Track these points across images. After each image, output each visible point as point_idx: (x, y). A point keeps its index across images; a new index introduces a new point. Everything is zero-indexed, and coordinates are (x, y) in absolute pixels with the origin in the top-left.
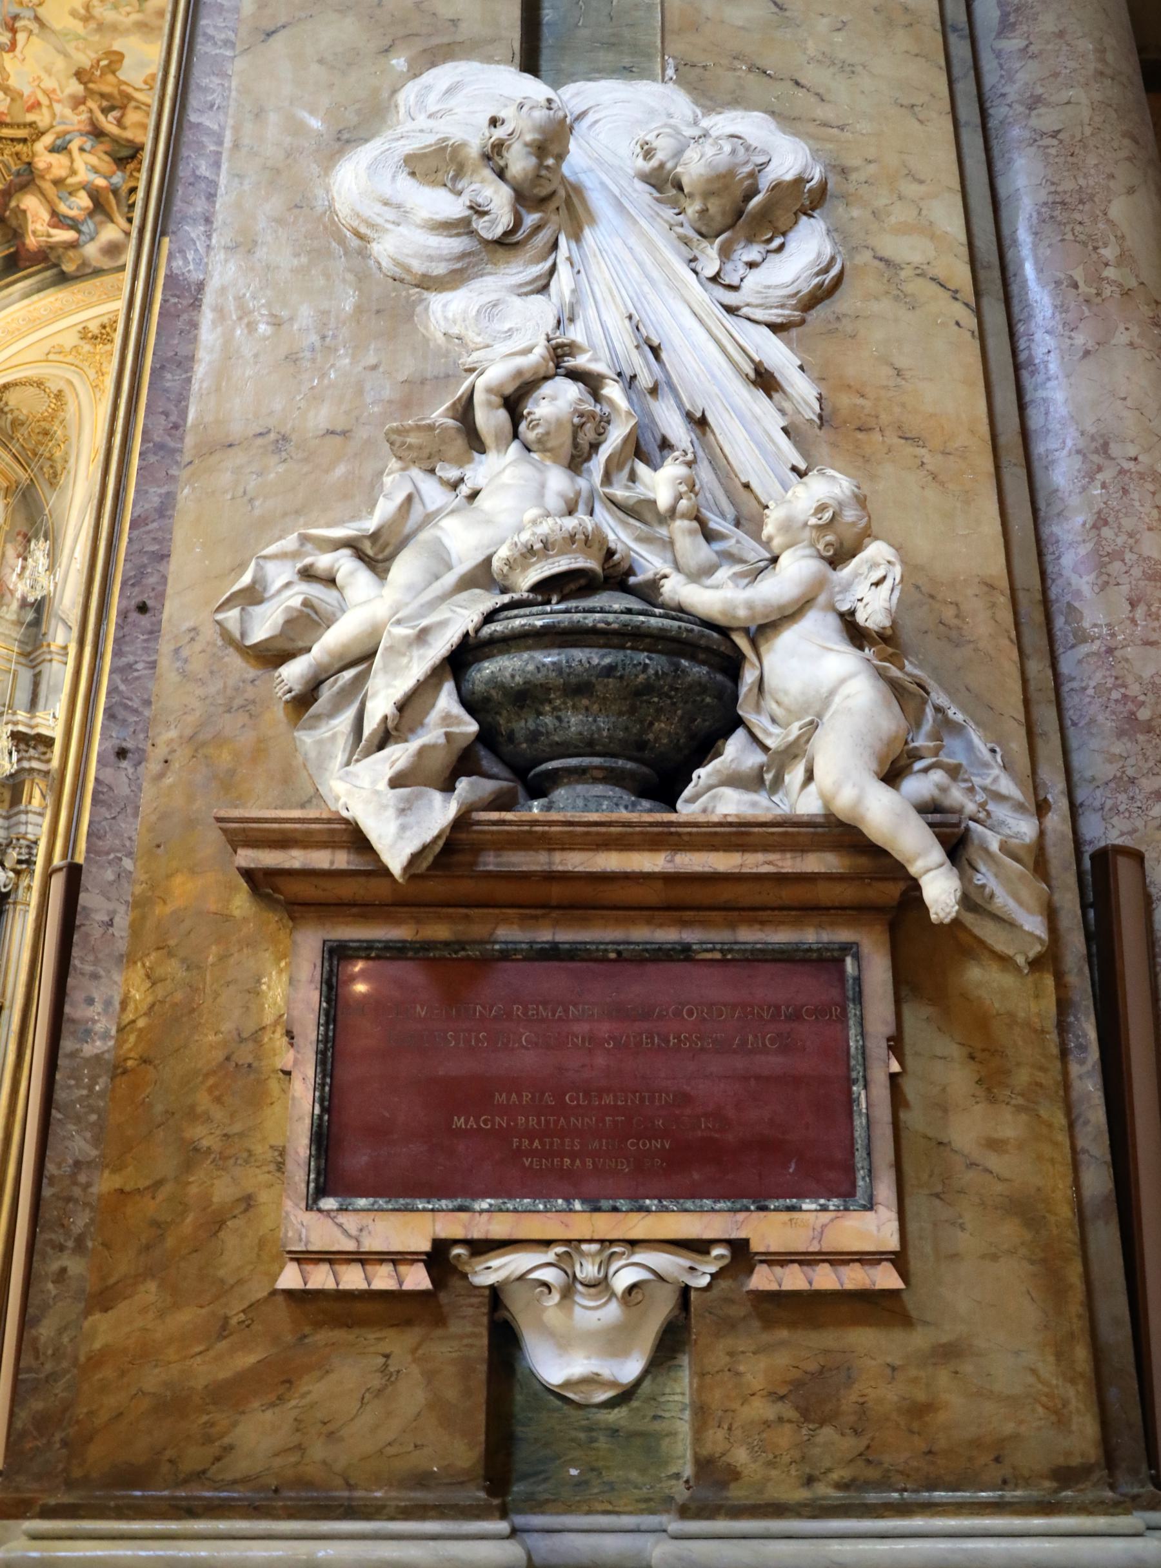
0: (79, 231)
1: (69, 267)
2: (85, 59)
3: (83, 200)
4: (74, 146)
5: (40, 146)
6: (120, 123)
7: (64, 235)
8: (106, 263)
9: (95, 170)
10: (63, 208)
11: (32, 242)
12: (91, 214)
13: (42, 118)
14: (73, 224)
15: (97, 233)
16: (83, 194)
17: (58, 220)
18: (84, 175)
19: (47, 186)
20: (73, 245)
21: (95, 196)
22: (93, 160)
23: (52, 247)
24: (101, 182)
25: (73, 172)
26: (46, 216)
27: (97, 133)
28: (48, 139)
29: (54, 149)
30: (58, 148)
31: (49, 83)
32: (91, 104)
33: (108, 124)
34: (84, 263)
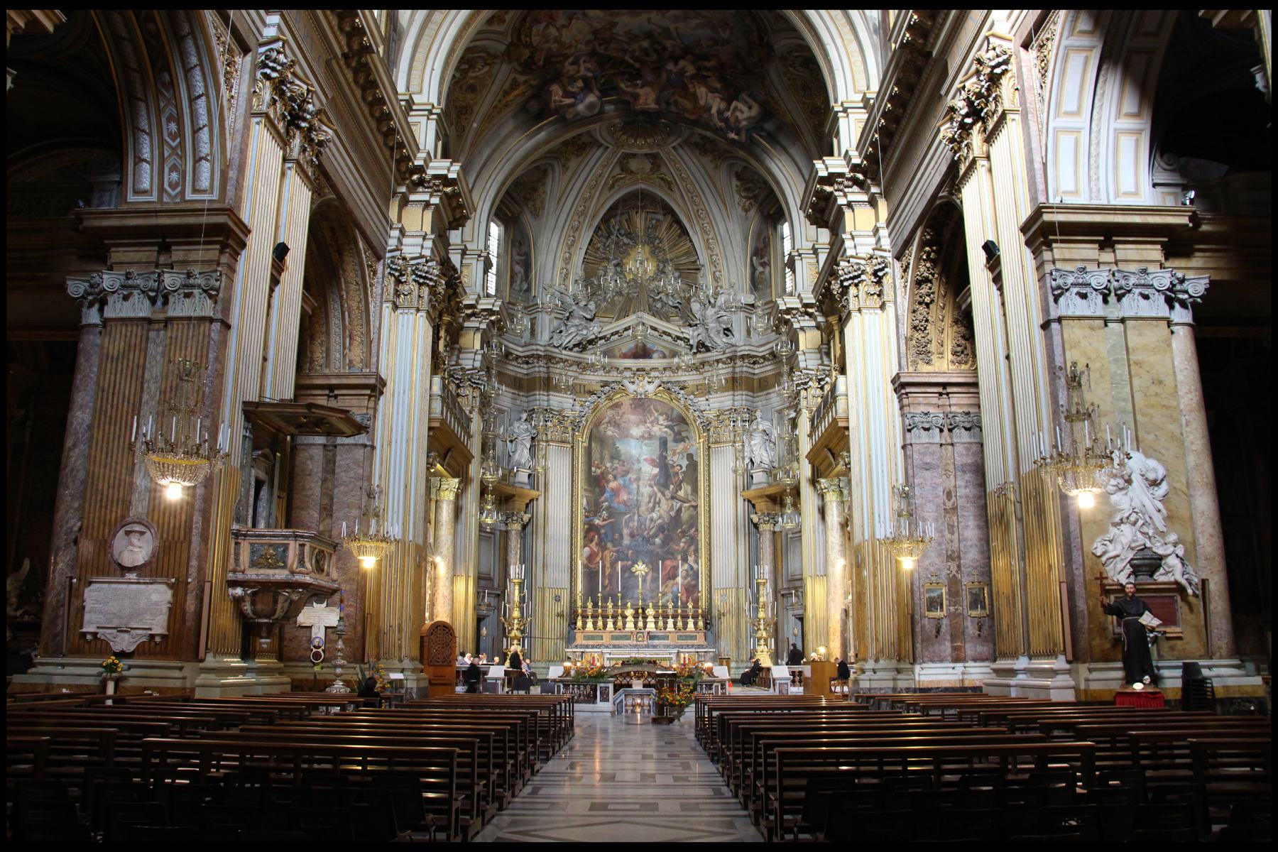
0: (575, 98)
1: (569, 116)
2: (598, 26)
3: (580, 84)
4: (581, 61)
5: (566, 64)
6: (606, 49)
7: (569, 101)
8: (588, 114)
9: (588, 70)
10: (570, 88)
11: (553, 105)
12: (582, 89)
13: (569, 52)
14: (573, 95)
15: (584, 98)
16: (580, 81)
17: (567, 94)
18: (583, 72)
19: (565, 80)
20: (572, 105)
21: (586, 80)
22: (588, 65)
23: (562, 107)
24: (590, 75)
25: (578, 72)
26: (561, 93)
27: (593, 53)
28: (570, 60)
29: (571, 64)
30: (576, 63)
31: (579, 37)
32: (596, 43)
33: (601, 50)
34: (577, 114)
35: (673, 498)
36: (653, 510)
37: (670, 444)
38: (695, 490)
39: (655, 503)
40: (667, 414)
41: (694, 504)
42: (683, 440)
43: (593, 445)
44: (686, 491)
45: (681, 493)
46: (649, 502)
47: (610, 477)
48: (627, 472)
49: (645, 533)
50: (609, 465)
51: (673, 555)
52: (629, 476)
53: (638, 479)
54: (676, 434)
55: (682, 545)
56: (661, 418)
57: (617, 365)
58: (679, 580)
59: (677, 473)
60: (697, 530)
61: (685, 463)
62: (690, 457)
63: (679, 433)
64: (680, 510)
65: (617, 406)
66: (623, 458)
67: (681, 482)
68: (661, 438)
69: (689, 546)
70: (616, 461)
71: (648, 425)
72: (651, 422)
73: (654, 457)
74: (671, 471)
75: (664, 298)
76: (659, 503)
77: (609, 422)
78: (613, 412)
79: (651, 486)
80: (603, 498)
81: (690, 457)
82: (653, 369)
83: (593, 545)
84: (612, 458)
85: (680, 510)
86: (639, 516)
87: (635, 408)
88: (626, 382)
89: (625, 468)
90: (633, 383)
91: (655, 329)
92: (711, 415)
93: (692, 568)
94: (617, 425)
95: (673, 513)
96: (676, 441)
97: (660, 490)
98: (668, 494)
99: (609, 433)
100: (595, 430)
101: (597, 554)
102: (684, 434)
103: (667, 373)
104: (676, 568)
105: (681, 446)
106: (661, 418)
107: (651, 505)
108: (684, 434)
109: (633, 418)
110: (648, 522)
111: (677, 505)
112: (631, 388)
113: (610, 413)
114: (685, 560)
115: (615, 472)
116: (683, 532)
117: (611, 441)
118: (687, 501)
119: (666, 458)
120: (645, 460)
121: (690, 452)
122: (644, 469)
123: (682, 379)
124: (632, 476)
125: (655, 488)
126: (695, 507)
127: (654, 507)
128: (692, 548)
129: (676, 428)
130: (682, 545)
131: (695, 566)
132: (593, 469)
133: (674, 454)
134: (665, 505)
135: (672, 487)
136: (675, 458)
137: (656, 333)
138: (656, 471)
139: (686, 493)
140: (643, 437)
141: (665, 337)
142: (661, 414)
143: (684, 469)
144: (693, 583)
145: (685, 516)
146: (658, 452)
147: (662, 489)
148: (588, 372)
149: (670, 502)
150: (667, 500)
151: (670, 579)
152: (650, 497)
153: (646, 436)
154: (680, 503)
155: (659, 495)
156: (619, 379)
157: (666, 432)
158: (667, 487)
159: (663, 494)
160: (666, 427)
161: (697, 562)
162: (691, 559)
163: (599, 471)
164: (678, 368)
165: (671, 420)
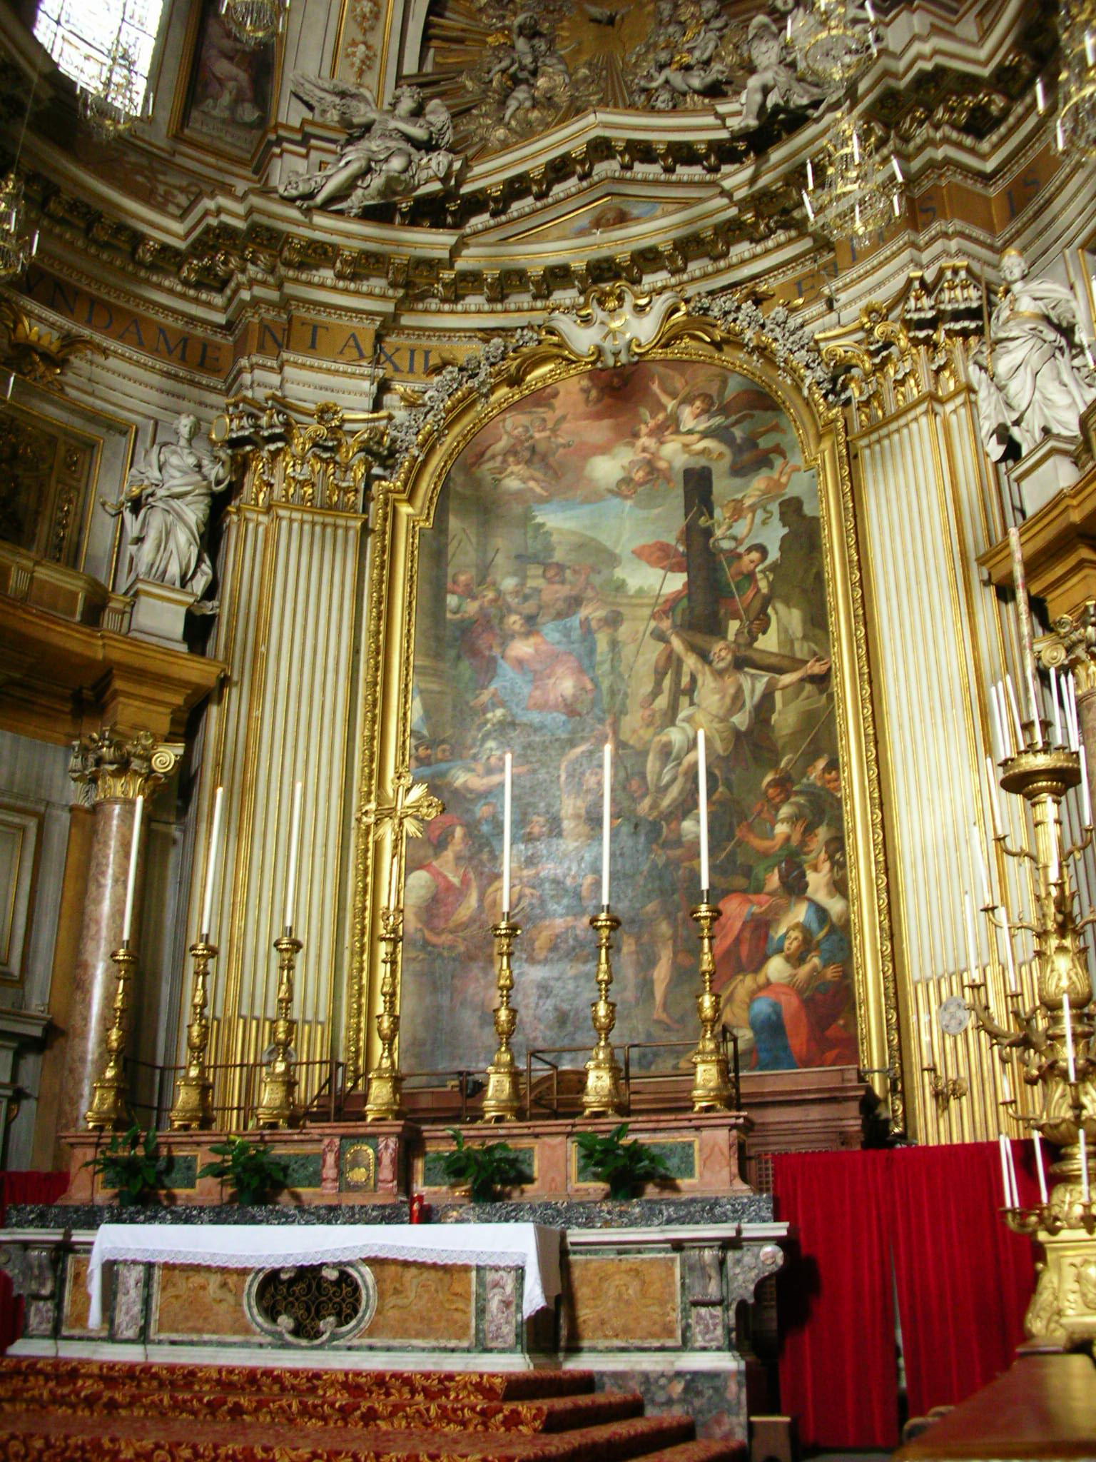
35: (740, 663)
36: (670, 716)
37: (722, 486)
38: (818, 620)
39: (677, 693)
40: (707, 397)
41: (817, 669)
42: (764, 461)
43: (454, 523)
44: (783, 630)
45: (769, 642)
46: (656, 692)
47: (514, 621)
48: (575, 602)
49: (647, 802)
50: (509, 583)
51: (748, 872)
52: (584, 612)
53: (614, 620)
54: (738, 450)
55: (781, 829)
56: (687, 414)
57: (521, 262)
58: (776, 968)
59: (751, 576)
60: (833, 765)
61: (773, 535)
62: (792, 510)
63: (751, 442)
64: (765, 705)
65: (542, 398)
66: (558, 556)
67: (767, 600)
68: (689, 474)
69: (809, 830)
70: (534, 570)
71: (644, 441)
72: (651, 434)
73: (671, 539)
74: (729, 572)
75: (677, 79)
76: (691, 690)
77: (512, 451)
78: (523, 419)
79: (660, 637)
80: (485, 697)
81: (792, 510)
82: (648, 259)
83: (449, 854)
84: (523, 559)
85: (765, 705)
86: (620, 745)
87: (599, 400)
88: (565, 324)
89: (564, 591)
90: (587, 321)
91: (643, 152)
92: (843, 347)
93: (822, 913)
94: (534, 455)
95: (741, 720)
96: (738, 471)
97: (692, 648)
98: (721, 652)
99: (512, 484)
100: (459, 479)
101: (460, 893)
102: (763, 443)
103: (695, 267)
104: (761, 927)
105: (759, 483)
106: (687, 414)
107: (662, 702)
108: (763, 443)
109: (598, 431)
110: (652, 764)
111: (754, 685)
112: (583, 339)
113: (514, 424)
114: (795, 887)
115: (530, 607)
116: (784, 784)
117: (518, 509)
118: (792, 663)
119: (708, 533)
120: (639, 554)
121: (791, 492)
122: (633, 584)
123: (747, 271)
124: (592, 612)
125: (677, 644)
126: (822, 681)
127: (674, 708)
128: (822, 833)
129: (738, 433)
130: (781, 829)
131: (835, 906)
132: (452, 600)
133: (738, 512)
134: (711, 695)
135: (734, 626)
136: (741, 528)
137: (654, 170)
138: (676, 582)
139: (787, 640)
140: (627, 481)
141: (683, 172)
142: (688, 400)
143: (774, 555)
144: (831, 973)
145: (785, 718)
146: (680, 522)
147: (700, 640)
148: (434, 304)
149: (730, 683)
150: (719, 674)
151: (741, 969)
152: (660, 675)
153: (639, 475)
154: (765, 678)
155: (691, 662)
156: (538, 318)
157: (704, 452)
158: (716, 628)
159: (704, 656)
160: (705, 435)
161: (840, 887)
162: (817, 881)
163: (472, 607)
164: (732, 231)
165: (724, 410)
